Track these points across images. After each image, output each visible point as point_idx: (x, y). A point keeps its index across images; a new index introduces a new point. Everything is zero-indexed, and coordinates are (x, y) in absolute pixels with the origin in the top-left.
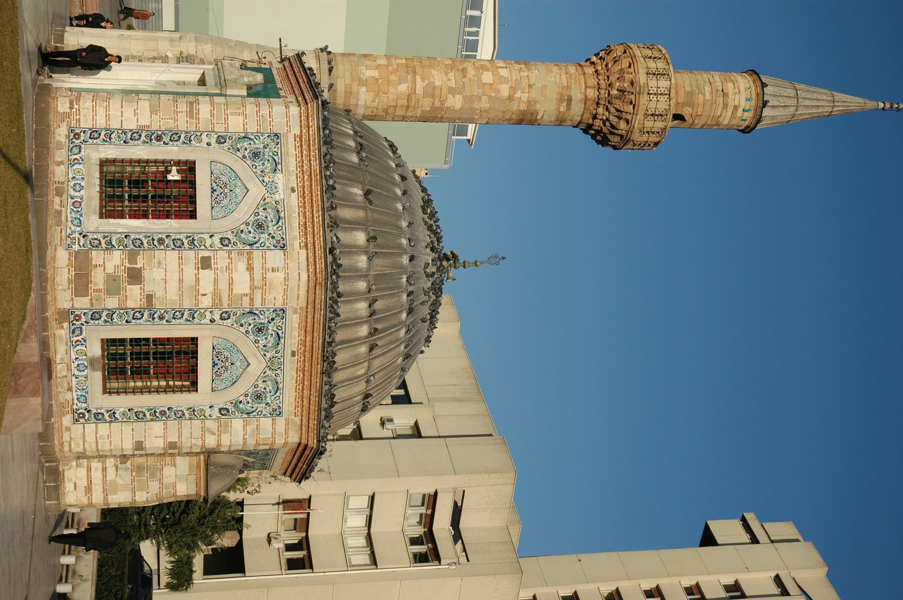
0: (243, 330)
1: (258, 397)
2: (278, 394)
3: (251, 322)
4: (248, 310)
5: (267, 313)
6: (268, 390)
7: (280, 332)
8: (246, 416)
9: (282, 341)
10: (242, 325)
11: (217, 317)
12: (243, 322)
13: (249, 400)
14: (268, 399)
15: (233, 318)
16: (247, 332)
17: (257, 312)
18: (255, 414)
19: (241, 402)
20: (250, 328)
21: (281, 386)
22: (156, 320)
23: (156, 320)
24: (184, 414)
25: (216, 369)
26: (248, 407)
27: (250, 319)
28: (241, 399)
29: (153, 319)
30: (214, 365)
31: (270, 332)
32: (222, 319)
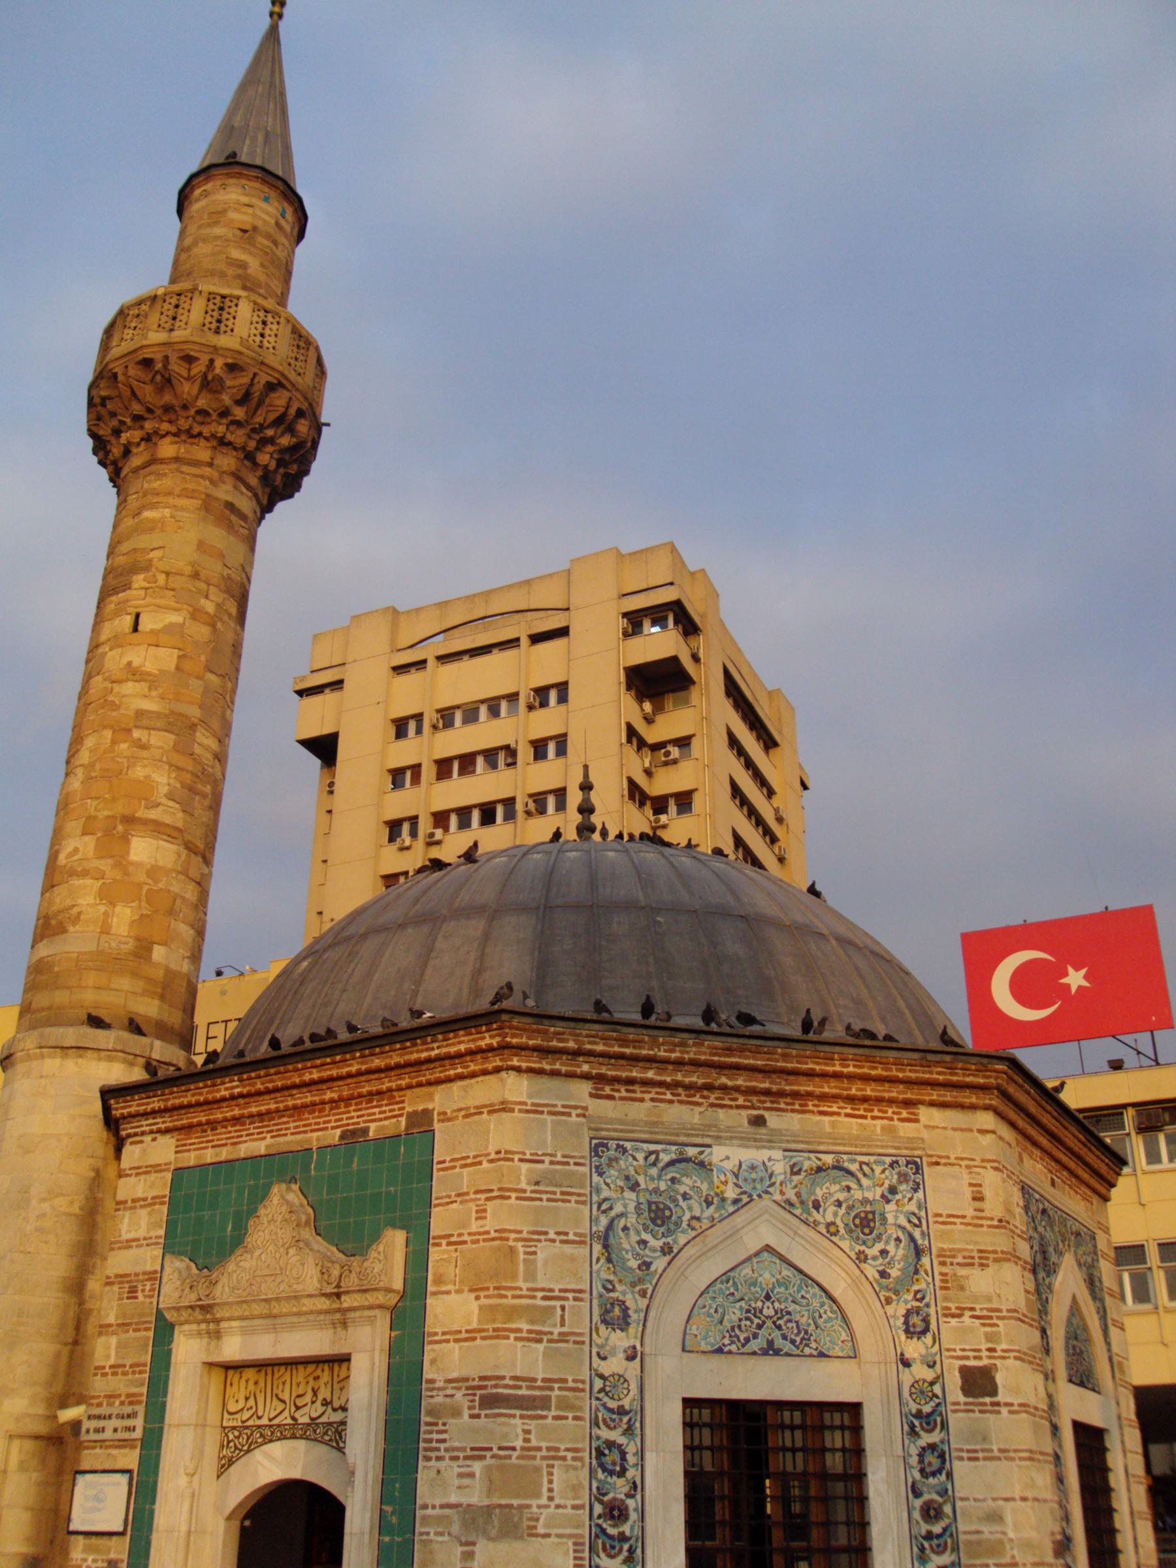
0: (659, 1264)
1: (866, 1223)
2: (854, 1167)
3: (634, 1238)
4: (597, 1248)
5: (606, 1193)
6: (841, 1196)
7: (665, 1158)
8: (925, 1260)
9: (691, 1152)
10: (647, 1265)
11: (620, 1340)
12: (633, 1264)
13: (874, 1251)
14: (869, 1195)
15: (622, 1291)
16: (666, 1250)
17: (604, 1221)
18: (917, 1234)
19: (883, 1274)
20: (654, 1243)
21: (829, 1159)
22: (626, 1528)
23: (626, 1528)
24: (932, 1447)
25: (787, 1347)
26: (898, 1252)
27: (626, 1243)
28: (871, 1271)
29: (623, 1538)
30: (771, 1350)
31: (663, 1186)
32: (624, 1323)
